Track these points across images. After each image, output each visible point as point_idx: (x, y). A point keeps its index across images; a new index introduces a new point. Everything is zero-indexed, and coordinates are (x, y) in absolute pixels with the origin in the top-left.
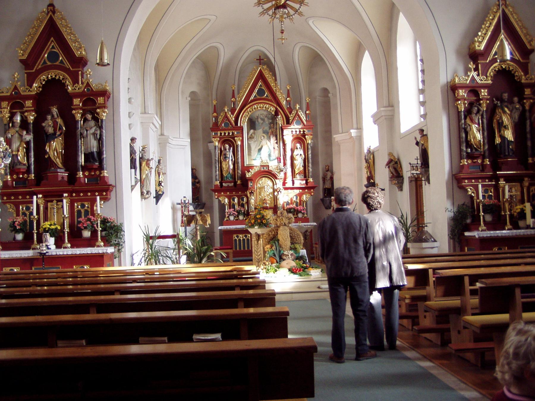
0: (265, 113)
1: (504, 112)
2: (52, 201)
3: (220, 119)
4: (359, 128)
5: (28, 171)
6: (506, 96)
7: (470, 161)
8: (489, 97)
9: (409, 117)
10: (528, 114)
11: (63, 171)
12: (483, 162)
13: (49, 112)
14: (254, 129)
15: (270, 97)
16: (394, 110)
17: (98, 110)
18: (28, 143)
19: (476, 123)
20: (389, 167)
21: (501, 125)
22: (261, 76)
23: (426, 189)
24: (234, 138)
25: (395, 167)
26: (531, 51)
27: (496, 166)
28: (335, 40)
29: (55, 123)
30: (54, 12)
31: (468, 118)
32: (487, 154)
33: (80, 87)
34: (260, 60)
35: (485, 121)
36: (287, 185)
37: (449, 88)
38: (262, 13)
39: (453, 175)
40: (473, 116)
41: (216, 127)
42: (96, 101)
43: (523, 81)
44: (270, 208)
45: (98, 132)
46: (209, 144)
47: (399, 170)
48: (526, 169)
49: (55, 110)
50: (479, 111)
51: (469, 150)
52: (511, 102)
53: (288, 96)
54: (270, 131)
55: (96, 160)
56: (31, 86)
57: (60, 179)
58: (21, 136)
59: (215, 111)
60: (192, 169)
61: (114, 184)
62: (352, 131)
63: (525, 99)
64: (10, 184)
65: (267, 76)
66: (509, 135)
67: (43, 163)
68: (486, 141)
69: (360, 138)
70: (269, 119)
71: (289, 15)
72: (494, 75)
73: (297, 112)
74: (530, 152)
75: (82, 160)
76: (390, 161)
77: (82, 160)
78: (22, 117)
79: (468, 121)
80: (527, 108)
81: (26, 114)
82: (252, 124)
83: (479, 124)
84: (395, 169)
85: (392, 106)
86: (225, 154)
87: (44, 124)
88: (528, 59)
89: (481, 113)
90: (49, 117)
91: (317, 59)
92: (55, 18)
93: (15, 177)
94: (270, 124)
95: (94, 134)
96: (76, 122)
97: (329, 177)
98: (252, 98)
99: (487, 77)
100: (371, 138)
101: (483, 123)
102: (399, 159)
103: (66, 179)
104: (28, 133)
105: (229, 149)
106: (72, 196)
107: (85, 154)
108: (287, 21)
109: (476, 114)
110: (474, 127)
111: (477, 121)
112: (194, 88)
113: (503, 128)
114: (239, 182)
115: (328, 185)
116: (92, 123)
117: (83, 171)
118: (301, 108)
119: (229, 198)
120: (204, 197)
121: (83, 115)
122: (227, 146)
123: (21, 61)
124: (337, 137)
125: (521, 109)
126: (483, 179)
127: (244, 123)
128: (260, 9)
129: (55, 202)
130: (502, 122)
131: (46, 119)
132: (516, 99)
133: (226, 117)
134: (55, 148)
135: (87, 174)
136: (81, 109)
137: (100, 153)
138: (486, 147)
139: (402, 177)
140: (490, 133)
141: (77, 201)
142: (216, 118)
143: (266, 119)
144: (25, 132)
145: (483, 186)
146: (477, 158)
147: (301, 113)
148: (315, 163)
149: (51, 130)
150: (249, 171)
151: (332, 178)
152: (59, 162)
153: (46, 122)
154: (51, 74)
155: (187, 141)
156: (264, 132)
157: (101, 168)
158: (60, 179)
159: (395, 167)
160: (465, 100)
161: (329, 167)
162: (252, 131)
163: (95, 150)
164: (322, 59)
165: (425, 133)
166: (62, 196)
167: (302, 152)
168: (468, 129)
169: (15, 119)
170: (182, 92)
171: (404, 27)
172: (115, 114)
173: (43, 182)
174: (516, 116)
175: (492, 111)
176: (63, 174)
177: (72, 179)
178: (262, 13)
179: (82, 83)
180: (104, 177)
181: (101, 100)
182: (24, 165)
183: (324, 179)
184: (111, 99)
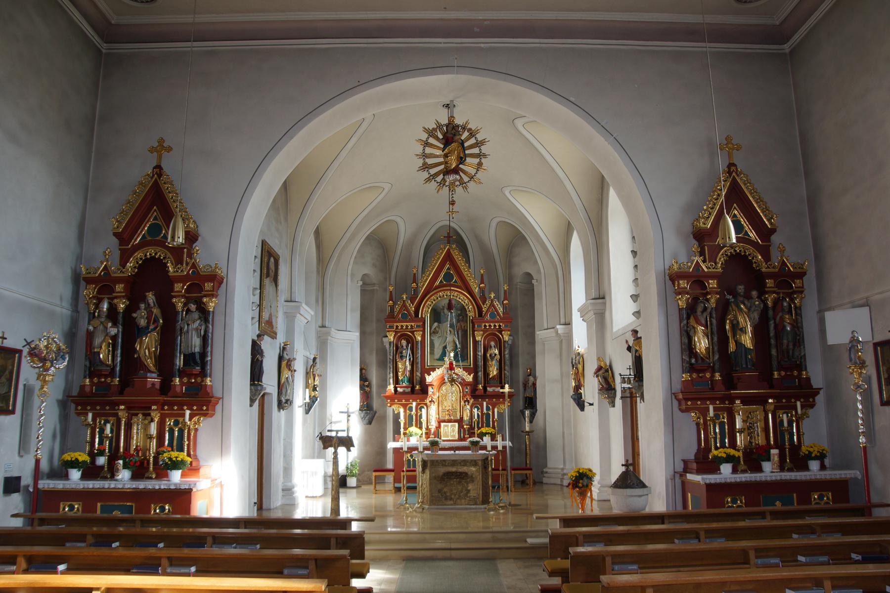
1: (741, 310)
2: (137, 415)
3: (397, 308)
4: (568, 324)
5: (112, 374)
6: (741, 289)
7: (695, 376)
9: (622, 314)
10: (771, 313)
11: (154, 375)
12: (713, 376)
13: (144, 299)
14: (439, 322)
15: (459, 283)
16: (605, 304)
17: (205, 300)
18: (114, 338)
20: (597, 376)
21: (735, 327)
22: (449, 257)
23: (641, 407)
24: (413, 332)
25: (605, 374)
26: (773, 231)
27: (730, 382)
28: (538, 215)
29: (150, 313)
30: (160, 175)
31: (692, 318)
32: (717, 366)
33: (185, 270)
35: (714, 321)
37: (667, 278)
38: (428, 180)
39: (675, 395)
40: (699, 313)
41: (391, 317)
42: (205, 285)
43: (764, 270)
44: (455, 421)
45: (203, 327)
46: (385, 340)
47: (610, 380)
48: (771, 387)
49: (151, 297)
50: (705, 309)
51: (693, 361)
52: (748, 297)
53: (482, 282)
55: (199, 363)
56: (124, 266)
57: (149, 386)
58: (106, 328)
59: (391, 299)
60: (361, 370)
61: (219, 395)
62: (558, 327)
63: (767, 293)
64: (87, 389)
65: (455, 257)
66: (747, 340)
67: (131, 364)
68: (716, 348)
69: (569, 337)
70: (457, 309)
71: (462, 182)
72: (726, 261)
73: (492, 301)
74: (775, 364)
75: (179, 362)
76: (600, 368)
77: (179, 362)
78: (110, 304)
79: (692, 321)
80: (770, 303)
81: (116, 301)
82: (437, 316)
83: (706, 326)
84: (606, 379)
85: (603, 298)
86: (401, 353)
87: (134, 315)
88: (769, 241)
89: (709, 310)
90: (142, 306)
91: (517, 239)
92: (161, 183)
93: (95, 380)
95: (197, 329)
96: (177, 313)
97: (531, 383)
98: (437, 283)
99: (716, 263)
100: (581, 337)
101: (711, 324)
102: (611, 366)
103: (158, 386)
104: (115, 324)
105: (407, 346)
106: (163, 409)
107: (185, 356)
108: (459, 190)
109: (702, 312)
110: (700, 328)
111: (703, 322)
112: (368, 270)
113: (739, 332)
114: (418, 387)
115: (529, 394)
116: (196, 315)
117: (181, 377)
118: (497, 297)
119: (405, 406)
120: (375, 405)
121: (185, 304)
122: (404, 343)
123: (115, 234)
124: (540, 334)
125: (762, 306)
126: (713, 400)
127: (426, 312)
128: (425, 175)
129: (140, 416)
130: (738, 322)
131: (139, 308)
132: (754, 293)
133: (404, 305)
134: (147, 346)
135: (185, 380)
136: (183, 296)
137: (203, 354)
138: (717, 357)
139: (614, 389)
140: (720, 339)
141: (171, 416)
142: (392, 308)
144: (110, 325)
145: (715, 409)
146: (703, 371)
147: (496, 303)
148: (513, 365)
149: (143, 322)
150: (429, 374)
151: (534, 384)
152: (150, 363)
153: (138, 312)
154: (150, 252)
155: (355, 336)
157: (203, 374)
158: (149, 386)
159: (605, 374)
160: (687, 293)
162: (436, 324)
163: (197, 350)
164: (525, 238)
165: (639, 335)
166: (150, 408)
167: (497, 352)
168: (691, 333)
169: (101, 306)
170: (353, 275)
171: (614, 200)
172: (227, 303)
173: (128, 390)
174: (756, 315)
175: (724, 309)
176: (153, 379)
177: (166, 387)
178: (428, 180)
179: (187, 264)
180: (206, 385)
181: (208, 286)
182: (107, 365)
183: (525, 385)
184: (223, 285)
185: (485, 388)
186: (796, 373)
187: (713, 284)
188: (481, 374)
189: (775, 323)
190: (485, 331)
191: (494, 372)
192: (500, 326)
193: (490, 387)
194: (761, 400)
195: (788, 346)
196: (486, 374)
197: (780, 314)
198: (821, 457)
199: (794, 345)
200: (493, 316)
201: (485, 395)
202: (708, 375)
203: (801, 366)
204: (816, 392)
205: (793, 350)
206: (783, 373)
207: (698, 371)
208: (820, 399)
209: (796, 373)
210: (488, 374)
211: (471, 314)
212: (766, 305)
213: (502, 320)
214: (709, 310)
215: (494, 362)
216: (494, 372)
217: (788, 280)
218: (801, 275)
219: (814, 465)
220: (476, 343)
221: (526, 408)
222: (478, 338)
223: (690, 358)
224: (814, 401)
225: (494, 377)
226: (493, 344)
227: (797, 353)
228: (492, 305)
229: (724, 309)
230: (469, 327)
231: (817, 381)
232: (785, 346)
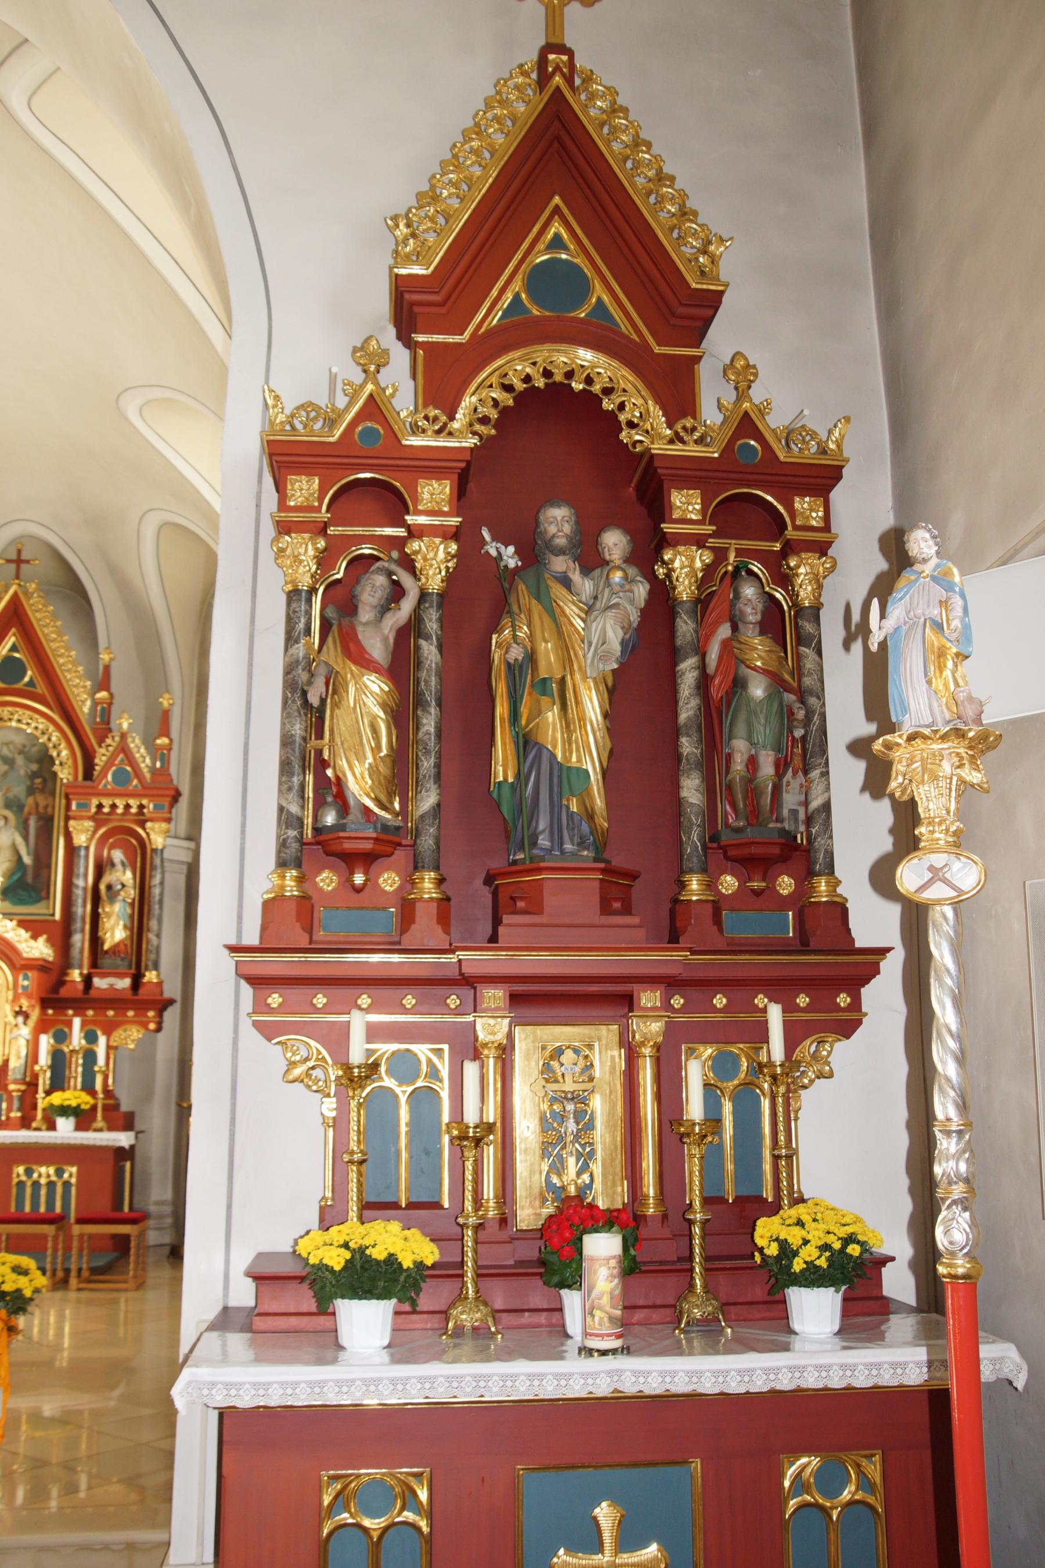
0: (19, 740)
6: (558, 521)
7: (327, 880)
8: (455, 521)
10: (685, 627)
15: (41, 688)
19: (365, 663)
34: (19, 561)
36: (64, 992)
40: (365, 615)
50: (397, 592)
51: (330, 818)
52: (591, 560)
54: (30, 801)
70: (29, 759)
73: (123, 736)
80: (685, 590)
89: (407, 605)
94: (33, 776)
125: (641, 591)
132: (614, 542)
143: (20, 760)
146: (367, 860)
156: (8, 806)
167: (128, 876)
185: (88, 980)
186: (786, 884)
187: (434, 493)
188: (80, 940)
189: (703, 666)
190: (99, 818)
192: (141, 807)
193: (103, 976)
194: (606, 998)
195: (752, 763)
196: (96, 941)
197: (724, 631)
198: (853, 1274)
199: (781, 766)
200: (121, 777)
201: (86, 1000)
202: (389, 881)
203: (802, 852)
204: (866, 965)
205: (777, 789)
206: (729, 883)
207: (351, 860)
208: (883, 997)
209: (786, 884)
211: (64, 775)
212: (662, 593)
213: (147, 790)
214: (407, 605)
215: (117, 907)
216: (115, 932)
217: (768, 492)
218: (822, 478)
219: (815, 1310)
220: (71, 851)
222: (80, 839)
223: (320, 804)
224: (856, 1005)
225: (115, 949)
226: (118, 855)
227: (790, 799)
228: (123, 749)
229: (478, 599)
230: (60, 802)
231: (873, 923)
232: (739, 765)
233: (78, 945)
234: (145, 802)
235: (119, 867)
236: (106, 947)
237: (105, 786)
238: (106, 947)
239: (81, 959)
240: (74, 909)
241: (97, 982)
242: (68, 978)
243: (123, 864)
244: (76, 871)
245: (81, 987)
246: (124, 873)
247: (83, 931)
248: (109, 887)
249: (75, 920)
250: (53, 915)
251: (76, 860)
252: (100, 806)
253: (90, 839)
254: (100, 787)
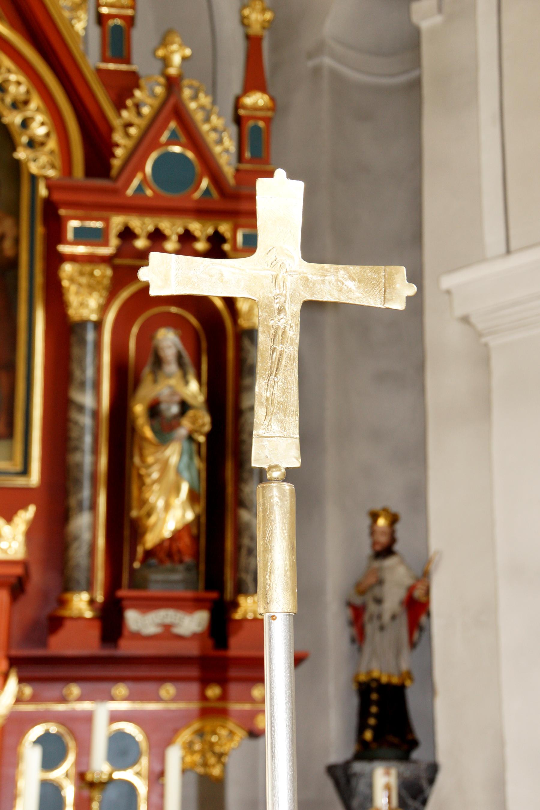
36: (61, 645)
73: (172, 84)
115: (382, 666)
151: (416, 609)
161: (394, 519)
167: (193, 390)
185: (110, 618)
188: (89, 526)
191: (170, 513)
193: (149, 604)
196: (123, 526)
210: (137, 531)
215: (173, 454)
220: (65, 334)
221: (365, 752)
228: (173, 109)
233: (86, 536)
234: (225, 228)
235: (172, 367)
236: (150, 540)
237: (140, 188)
238: (150, 540)
239: (91, 569)
240: (75, 458)
241: (135, 620)
242: (66, 613)
243: (180, 359)
244: (77, 373)
245: (94, 634)
246: (187, 383)
247: (93, 507)
248: (154, 410)
249: (78, 482)
250: (25, 471)
251: (75, 351)
252: (127, 234)
253: (104, 309)
254: (130, 192)
